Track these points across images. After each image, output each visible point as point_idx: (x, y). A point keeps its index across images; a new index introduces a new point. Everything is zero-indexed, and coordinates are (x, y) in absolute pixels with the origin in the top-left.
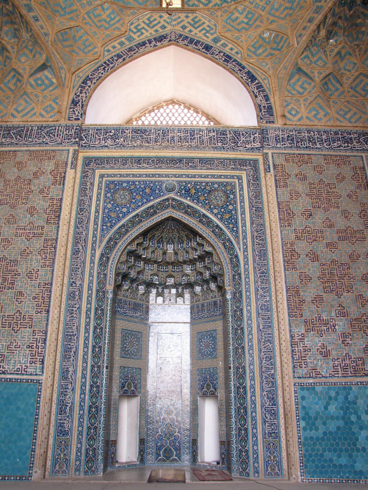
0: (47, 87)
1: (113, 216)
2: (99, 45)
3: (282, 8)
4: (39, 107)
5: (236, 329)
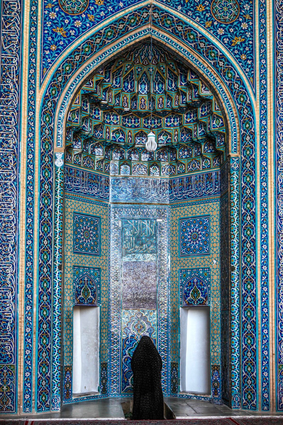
1: (59, 33)
5: (244, 215)
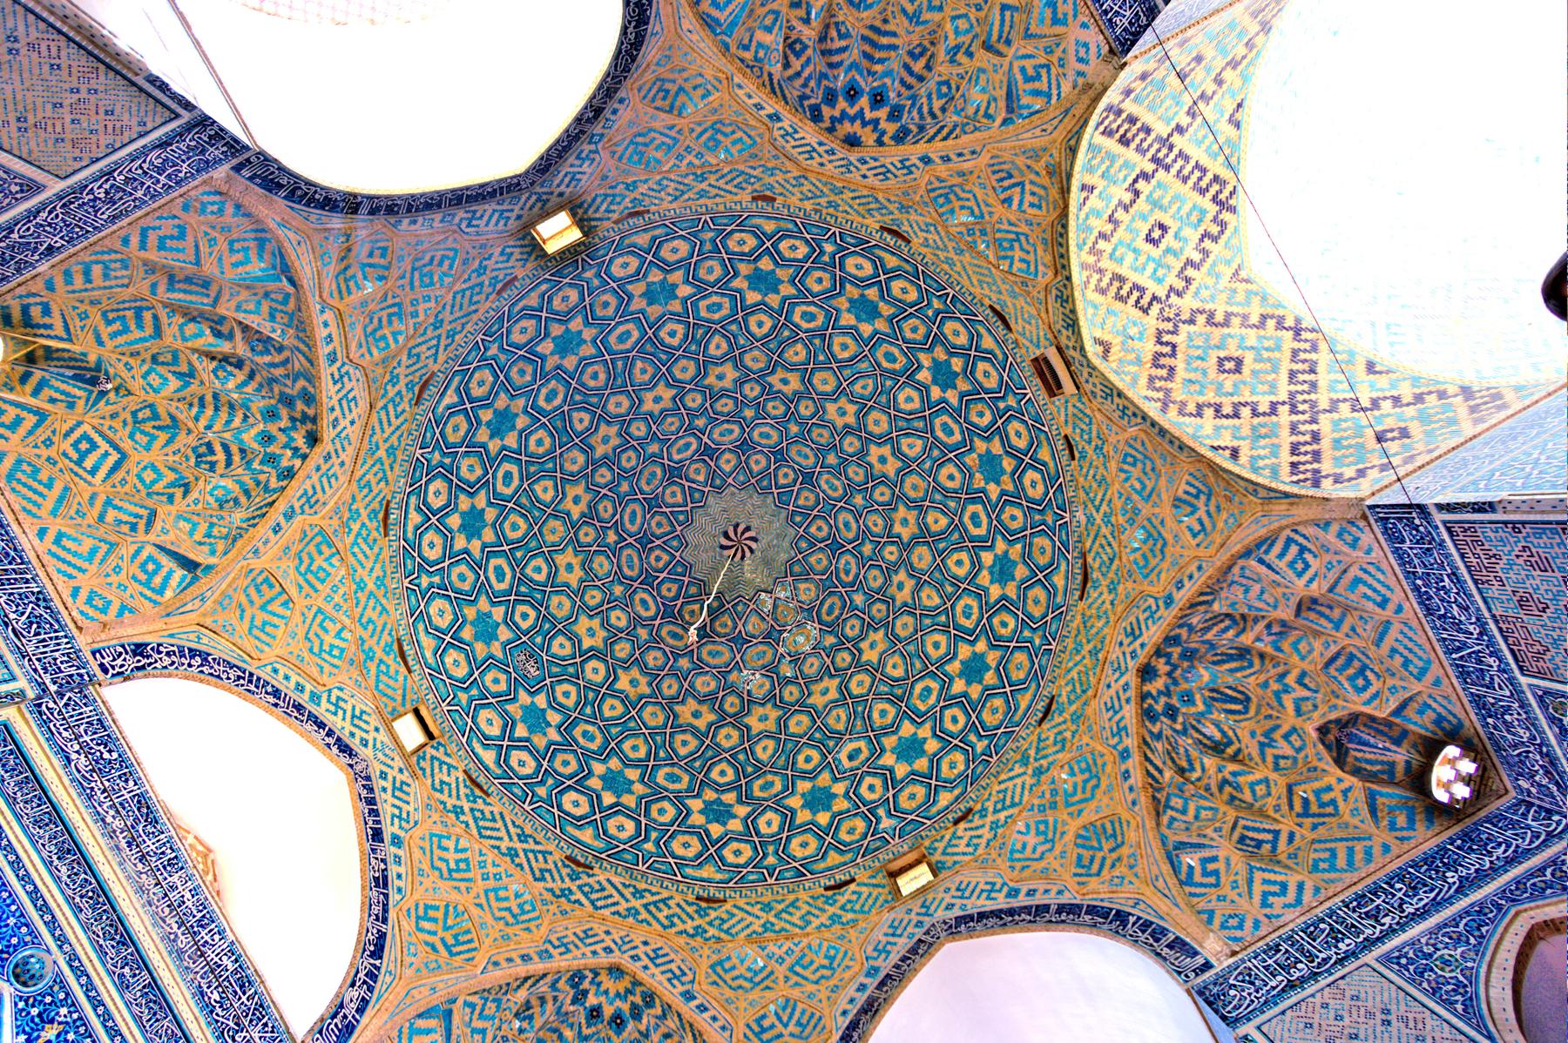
0: (147, 584)
2: (277, 651)
3: (505, 904)
4: (95, 581)
